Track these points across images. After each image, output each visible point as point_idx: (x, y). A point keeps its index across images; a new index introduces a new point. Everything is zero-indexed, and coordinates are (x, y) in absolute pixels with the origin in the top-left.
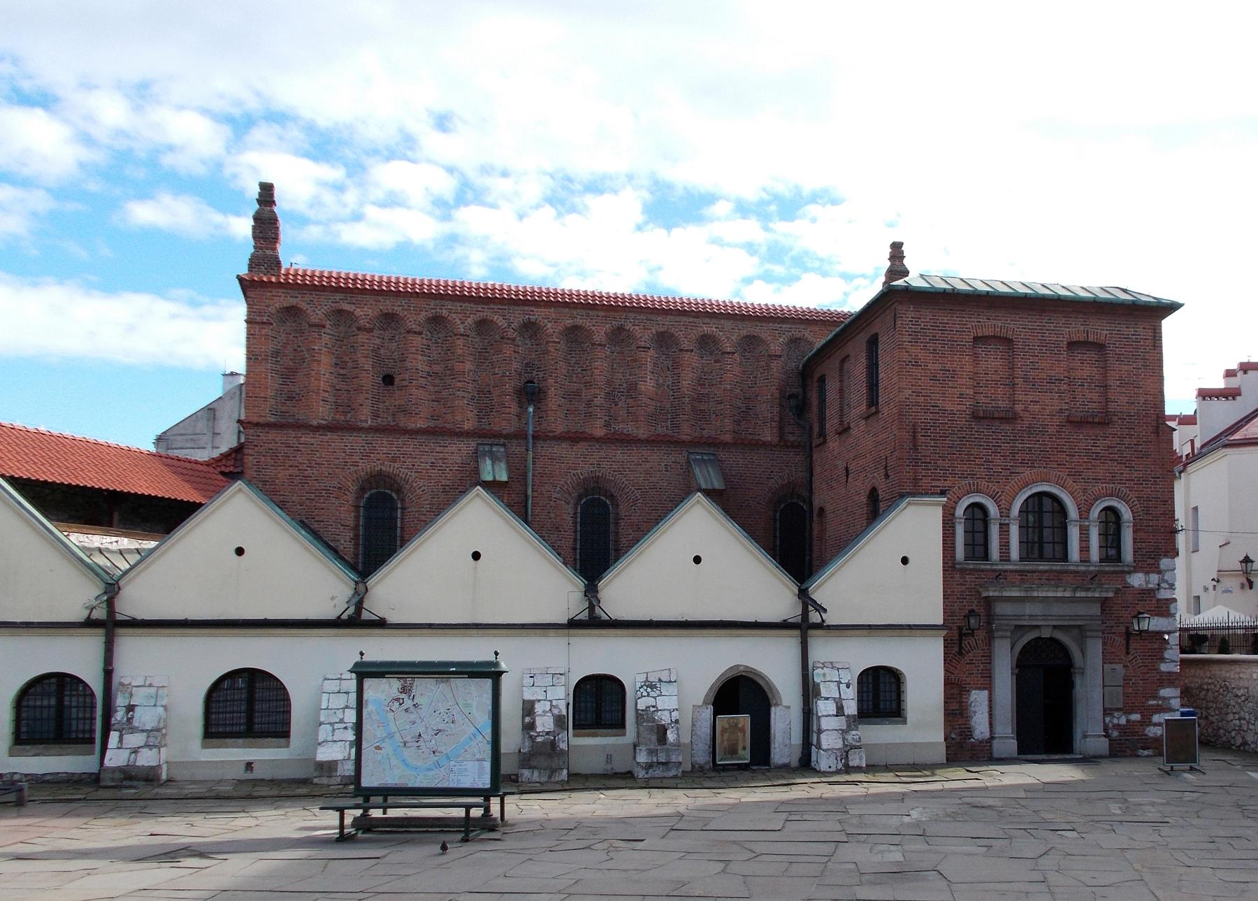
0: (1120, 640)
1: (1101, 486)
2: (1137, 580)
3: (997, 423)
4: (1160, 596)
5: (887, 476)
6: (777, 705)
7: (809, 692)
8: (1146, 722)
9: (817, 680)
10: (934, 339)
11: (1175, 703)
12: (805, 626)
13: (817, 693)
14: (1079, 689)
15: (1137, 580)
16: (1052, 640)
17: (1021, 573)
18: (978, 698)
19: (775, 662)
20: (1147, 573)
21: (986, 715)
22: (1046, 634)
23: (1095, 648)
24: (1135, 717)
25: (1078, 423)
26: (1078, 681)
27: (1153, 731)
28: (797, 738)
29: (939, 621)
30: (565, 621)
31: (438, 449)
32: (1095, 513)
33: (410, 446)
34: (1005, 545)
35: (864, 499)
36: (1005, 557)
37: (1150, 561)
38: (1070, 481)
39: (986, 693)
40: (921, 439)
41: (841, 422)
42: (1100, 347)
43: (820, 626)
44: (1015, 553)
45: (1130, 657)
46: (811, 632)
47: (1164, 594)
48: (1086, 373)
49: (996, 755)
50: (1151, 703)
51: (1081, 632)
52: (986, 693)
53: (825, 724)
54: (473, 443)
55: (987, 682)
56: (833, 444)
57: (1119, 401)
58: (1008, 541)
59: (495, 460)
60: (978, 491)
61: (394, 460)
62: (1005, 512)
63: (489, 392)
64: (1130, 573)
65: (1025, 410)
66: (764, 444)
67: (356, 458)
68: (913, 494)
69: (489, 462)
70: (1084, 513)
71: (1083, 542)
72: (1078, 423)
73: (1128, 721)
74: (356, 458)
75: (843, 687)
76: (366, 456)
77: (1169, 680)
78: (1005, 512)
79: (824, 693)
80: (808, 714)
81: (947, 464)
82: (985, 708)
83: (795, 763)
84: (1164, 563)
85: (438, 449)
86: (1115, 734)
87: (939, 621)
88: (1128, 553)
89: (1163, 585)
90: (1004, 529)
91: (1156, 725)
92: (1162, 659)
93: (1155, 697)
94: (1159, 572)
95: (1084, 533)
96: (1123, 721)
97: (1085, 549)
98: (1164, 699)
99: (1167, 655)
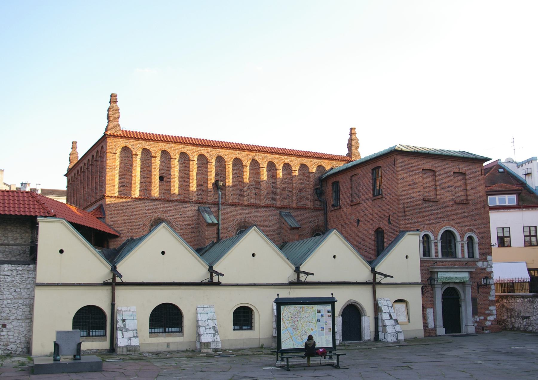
0: (476, 288)
1: (466, 228)
2: (480, 264)
3: (431, 203)
4: (488, 271)
5: (390, 223)
6: (365, 315)
7: (377, 309)
8: (485, 320)
9: (380, 305)
10: (409, 170)
11: (495, 312)
12: (373, 284)
13: (381, 311)
14: (463, 308)
15: (480, 264)
16: (453, 289)
17: (442, 261)
18: (430, 311)
19: (363, 298)
20: (483, 262)
21: (433, 318)
22: (451, 286)
23: (469, 291)
24: (482, 318)
25: (458, 204)
26: (463, 304)
27: (488, 323)
28: (373, 329)
29: (419, 281)
30: (287, 282)
31: (183, 209)
32: (465, 238)
33: (171, 207)
34: (436, 251)
35: (373, 233)
36: (437, 255)
37: (484, 257)
38: (456, 226)
39: (432, 309)
40: (406, 209)
41: (352, 201)
42: (464, 174)
43: (380, 283)
44: (440, 255)
45: (479, 294)
46: (377, 286)
47: (489, 270)
48: (459, 184)
49: (438, 334)
50: (487, 312)
51: (463, 284)
52: (432, 309)
53: (387, 323)
54: (197, 206)
55: (433, 306)
56: (346, 210)
57: (471, 196)
58: (437, 249)
59: (209, 214)
60: (426, 230)
61: (165, 213)
62: (436, 237)
63: (202, 185)
64: (477, 261)
65: (441, 198)
66: (308, 209)
67: (150, 212)
68: (409, 231)
69: (207, 215)
70: (462, 238)
71: (461, 250)
72: (458, 204)
73: (480, 319)
74: (150, 212)
75: (390, 308)
76: (154, 211)
77: (492, 303)
78: (436, 237)
79: (384, 311)
80: (376, 319)
81: (415, 219)
82: (432, 316)
83: (372, 339)
84: (489, 258)
85: (183, 209)
86: (476, 325)
87: (419, 281)
88: (477, 255)
89: (489, 266)
90: (436, 244)
91: (489, 321)
92: (490, 295)
93: (488, 310)
94: (487, 261)
95: (462, 245)
96: (478, 320)
97: (463, 253)
98: (491, 310)
99: (491, 293)
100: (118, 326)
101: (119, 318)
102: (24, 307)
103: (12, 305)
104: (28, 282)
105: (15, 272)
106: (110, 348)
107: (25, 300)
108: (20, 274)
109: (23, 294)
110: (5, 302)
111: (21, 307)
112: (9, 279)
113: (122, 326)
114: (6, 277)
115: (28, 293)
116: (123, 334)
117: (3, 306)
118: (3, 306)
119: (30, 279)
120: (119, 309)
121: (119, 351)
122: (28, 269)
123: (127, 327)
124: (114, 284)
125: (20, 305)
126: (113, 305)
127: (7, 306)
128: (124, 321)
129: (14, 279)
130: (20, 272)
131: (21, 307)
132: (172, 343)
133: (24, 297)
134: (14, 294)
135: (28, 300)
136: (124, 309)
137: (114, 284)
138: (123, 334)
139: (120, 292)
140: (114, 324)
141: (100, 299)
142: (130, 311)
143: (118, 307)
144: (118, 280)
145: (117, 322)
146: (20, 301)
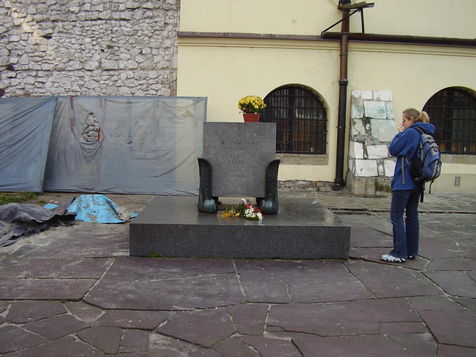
100: (354, 132)
101: (355, 113)
102: (160, 86)
103: (136, 83)
104: (165, 33)
105: (138, 14)
106: (336, 181)
107: (160, 72)
108: (148, 17)
109: (156, 59)
110: (123, 76)
111: (153, 87)
112: (127, 28)
113: (363, 133)
114: (123, 23)
115: (166, 58)
116: (365, 152)
117: (119, 83)
118: (119, 83)
119: (170, 27)
120: (356, 94)
121: (357, 188)
122: (165, 6)
123: (375, 135)
124: (344, 38)
125: (151, 82)
126: (343, 85)
127: (127, 83)
128: (366, 120)
129: (136, 27)
130: (149, 13)
131: (153, 87)
132: (466, 175)
133: (160, 66)
134: (140, 58)
135: (168, 72)
136: (366, 95)
137: (344, 38)
138: (365, 152)
139: (361, 59)
140: (344, 127)
141: (315, 71)
142: (378, 100)
143: (355, 90)
144: (355, 27)
145: (352, 122)
146: (152, 74)
